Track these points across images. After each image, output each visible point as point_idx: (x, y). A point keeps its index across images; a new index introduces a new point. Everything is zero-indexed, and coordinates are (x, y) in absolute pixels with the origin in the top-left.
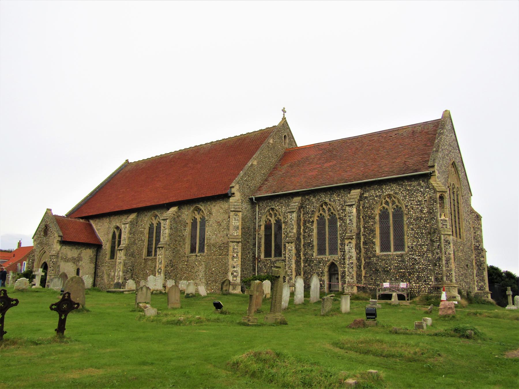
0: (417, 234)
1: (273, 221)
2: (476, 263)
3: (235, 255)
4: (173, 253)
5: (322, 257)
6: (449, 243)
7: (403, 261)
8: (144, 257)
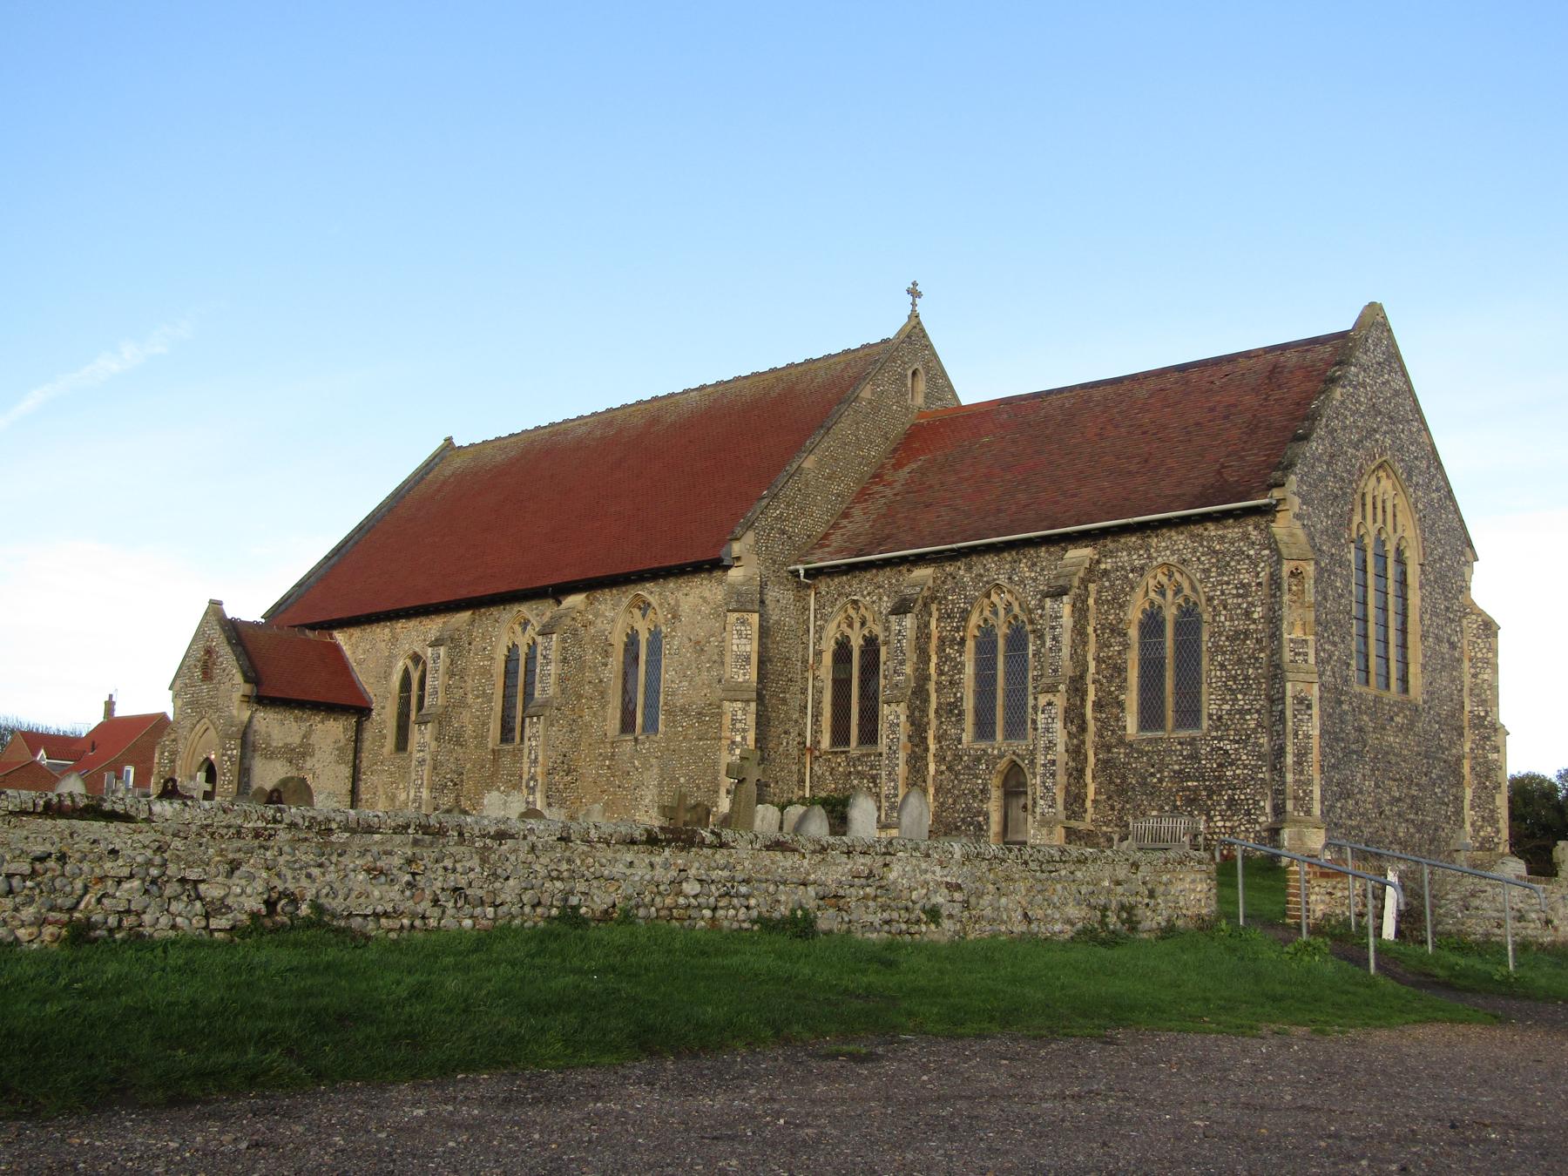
0: (1235, 678)
1: (856, 642)
2: (1473, 769)
3: (738, 739)
4: (572, 731)
6: (1309, 707)
7: (1195, 757)
8: (490, 746)
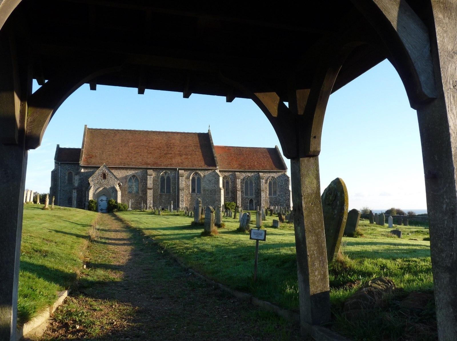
5: (247, 196)
7: (276, 199)
